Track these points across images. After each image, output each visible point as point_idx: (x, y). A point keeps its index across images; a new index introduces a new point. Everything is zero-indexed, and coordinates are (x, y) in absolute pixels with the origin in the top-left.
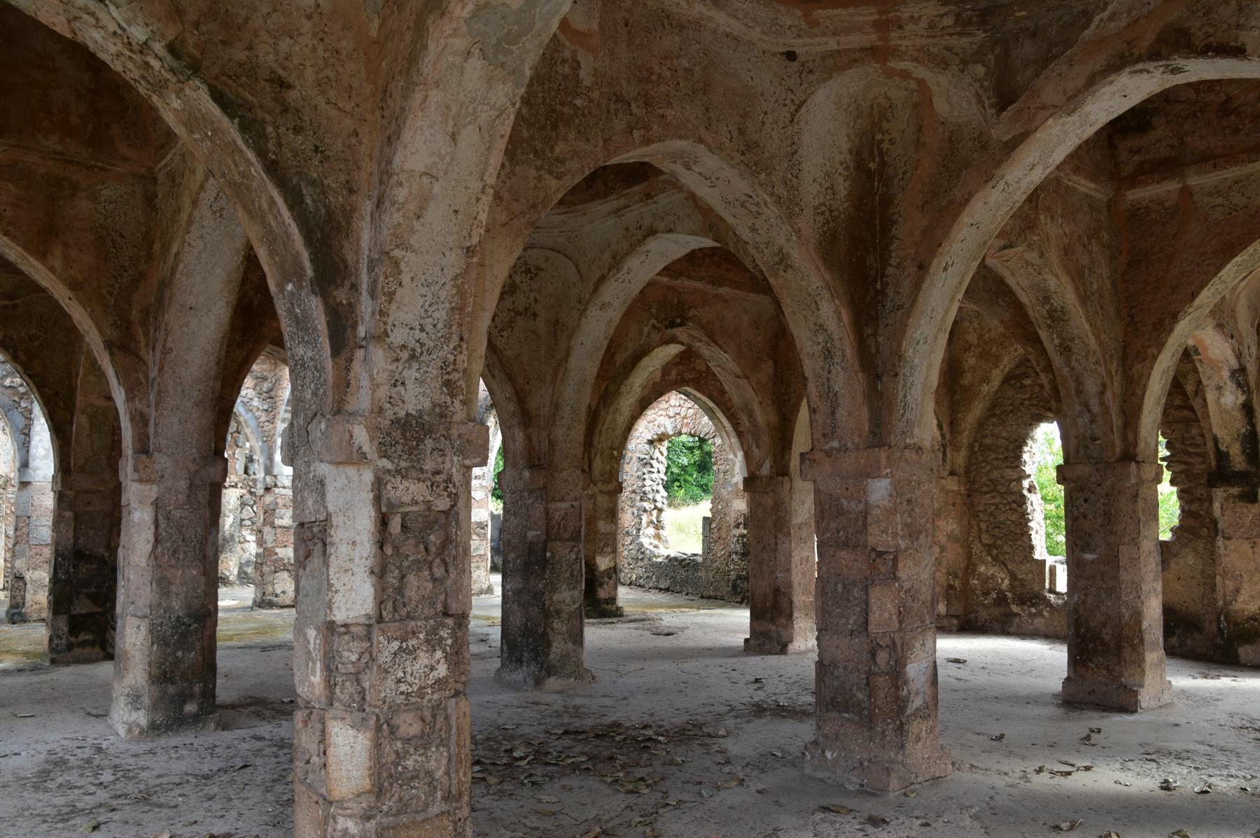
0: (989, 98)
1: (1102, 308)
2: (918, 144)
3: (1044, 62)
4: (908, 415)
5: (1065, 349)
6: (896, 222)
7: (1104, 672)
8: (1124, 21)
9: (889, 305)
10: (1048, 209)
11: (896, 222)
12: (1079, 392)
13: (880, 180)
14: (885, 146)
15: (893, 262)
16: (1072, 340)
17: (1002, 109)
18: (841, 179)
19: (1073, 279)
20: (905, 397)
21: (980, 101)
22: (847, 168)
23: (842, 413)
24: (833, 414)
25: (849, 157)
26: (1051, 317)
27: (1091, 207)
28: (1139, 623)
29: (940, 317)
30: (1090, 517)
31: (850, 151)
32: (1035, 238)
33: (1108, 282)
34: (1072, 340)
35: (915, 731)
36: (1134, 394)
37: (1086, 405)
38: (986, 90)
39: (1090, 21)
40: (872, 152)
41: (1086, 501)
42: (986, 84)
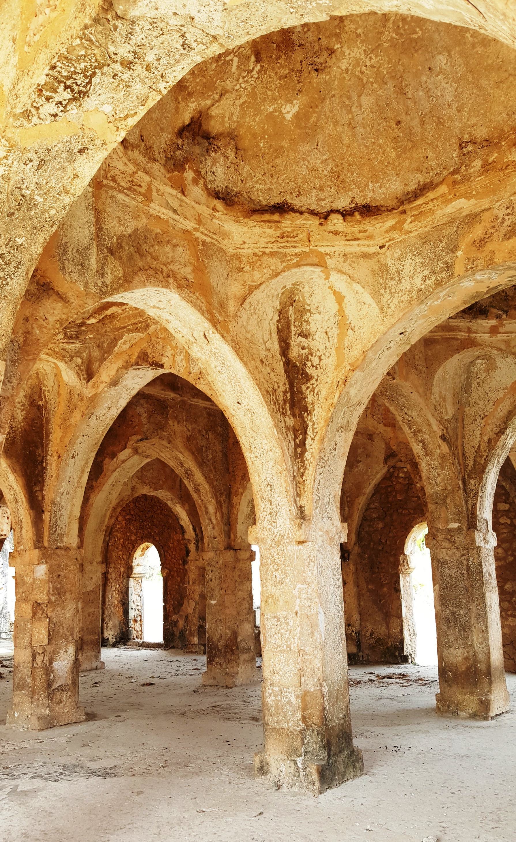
0: (83, 375)
1: (215, 468)
2: (59, 394)
3: (103, 360)
4: (59, 531)
5: (197, 490)
6: (51, 433)
7: (219, 666)
8: (128, 345)
9: (48, 475)
10: (176, 418)
11: (51, 433)
12: (207, 512)
13: (45, 411)
14: (46, 393)
15: (50, 453)
16: (199, 485)
17: (88, 381)
18: (19, 411)
19: (193, 453)
20: (56, 522)
21: (79, 376)
22: (23, 405)
23: (24, 531)
24: (21, 531)
25: (24, 400)
26: (186, 473)
27: (209, 414)
28: (236, 638)
29: (76, 481)
30: (213, 580)
31: (25, 396)
32: (165, 433)
33: (220, 455)
34: (199, 485)
35: (59, 698)
36: (233, 513)
37: (210, 519)
38: (82, 371)
39: (117, 343)
40: (40, 396)
41: (212, 571)
42: (82, 368)
